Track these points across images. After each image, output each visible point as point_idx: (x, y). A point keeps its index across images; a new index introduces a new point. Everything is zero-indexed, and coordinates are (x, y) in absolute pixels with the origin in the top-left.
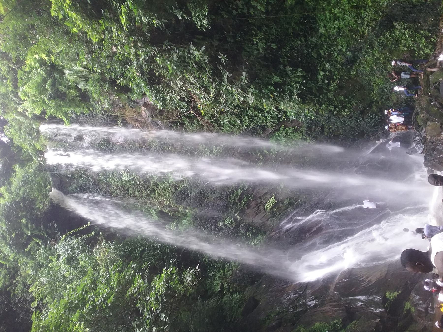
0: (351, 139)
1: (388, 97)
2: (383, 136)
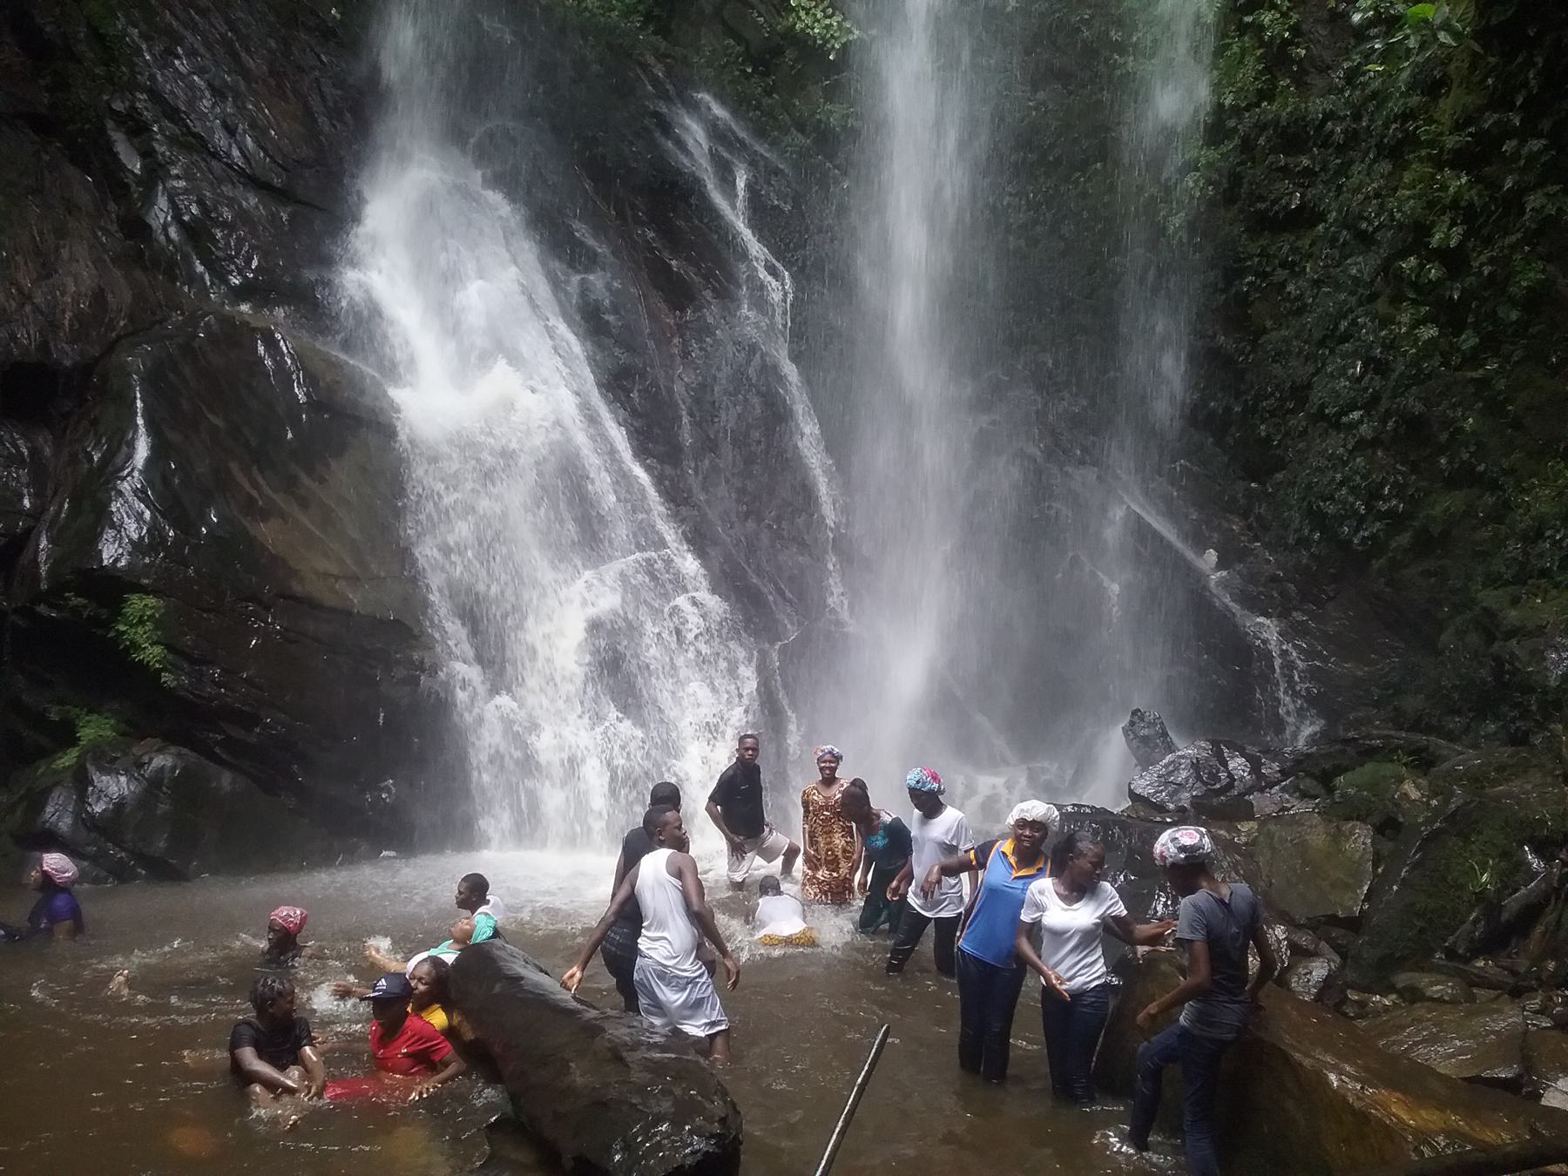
0: (1228, 409)
1: (1544, 573)
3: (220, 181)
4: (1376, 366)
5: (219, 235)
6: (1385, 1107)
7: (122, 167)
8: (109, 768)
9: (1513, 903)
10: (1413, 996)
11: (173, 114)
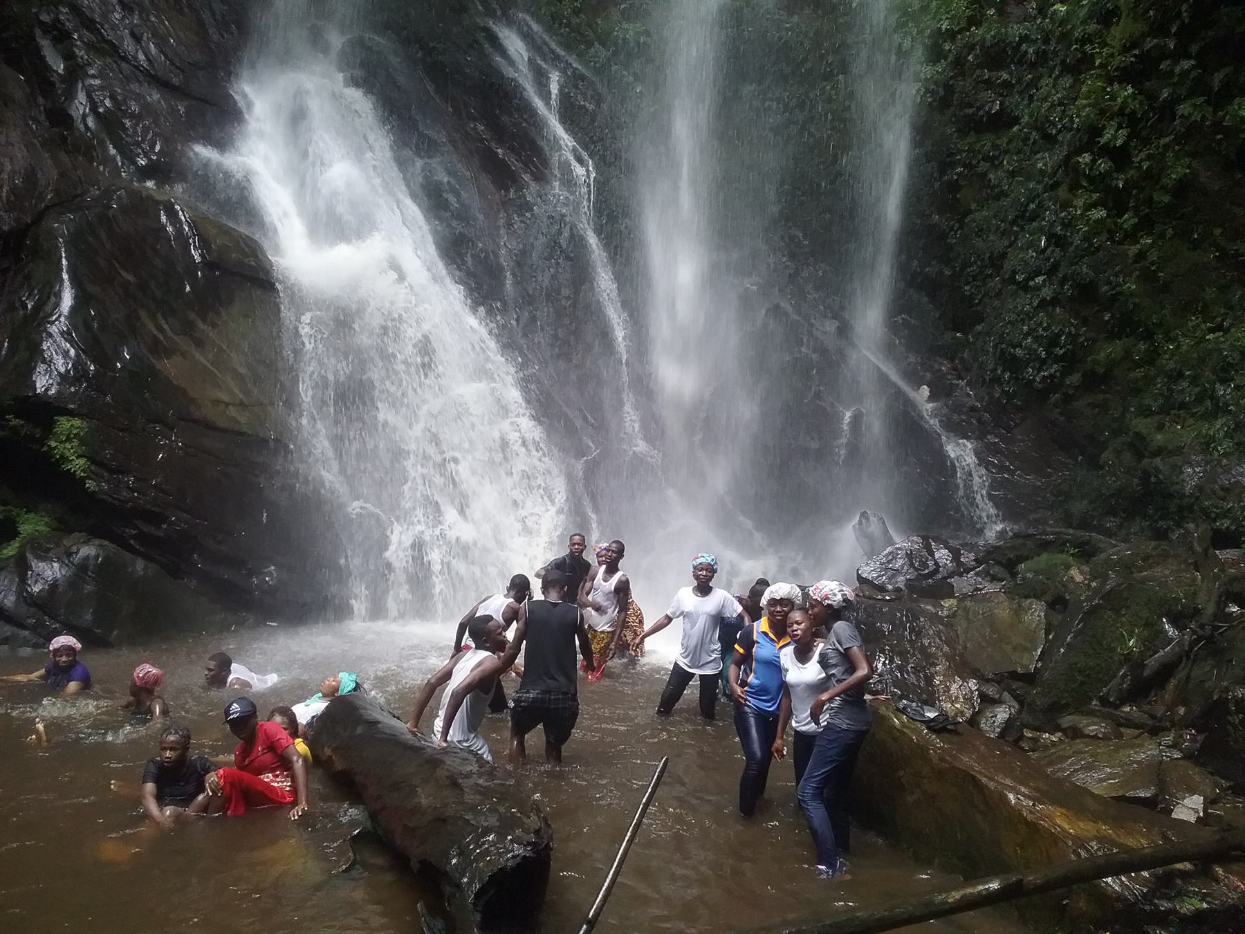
1: (1182, 406)
2: (957, 408)
3: (128, 79)
4: (1057, 241)
5: (128, 124)
6: (1050, 818)
7: (48, 68)
8: (44, 556)
9: (1153, 662)
10: (1075, 733)
11: (89, 24)
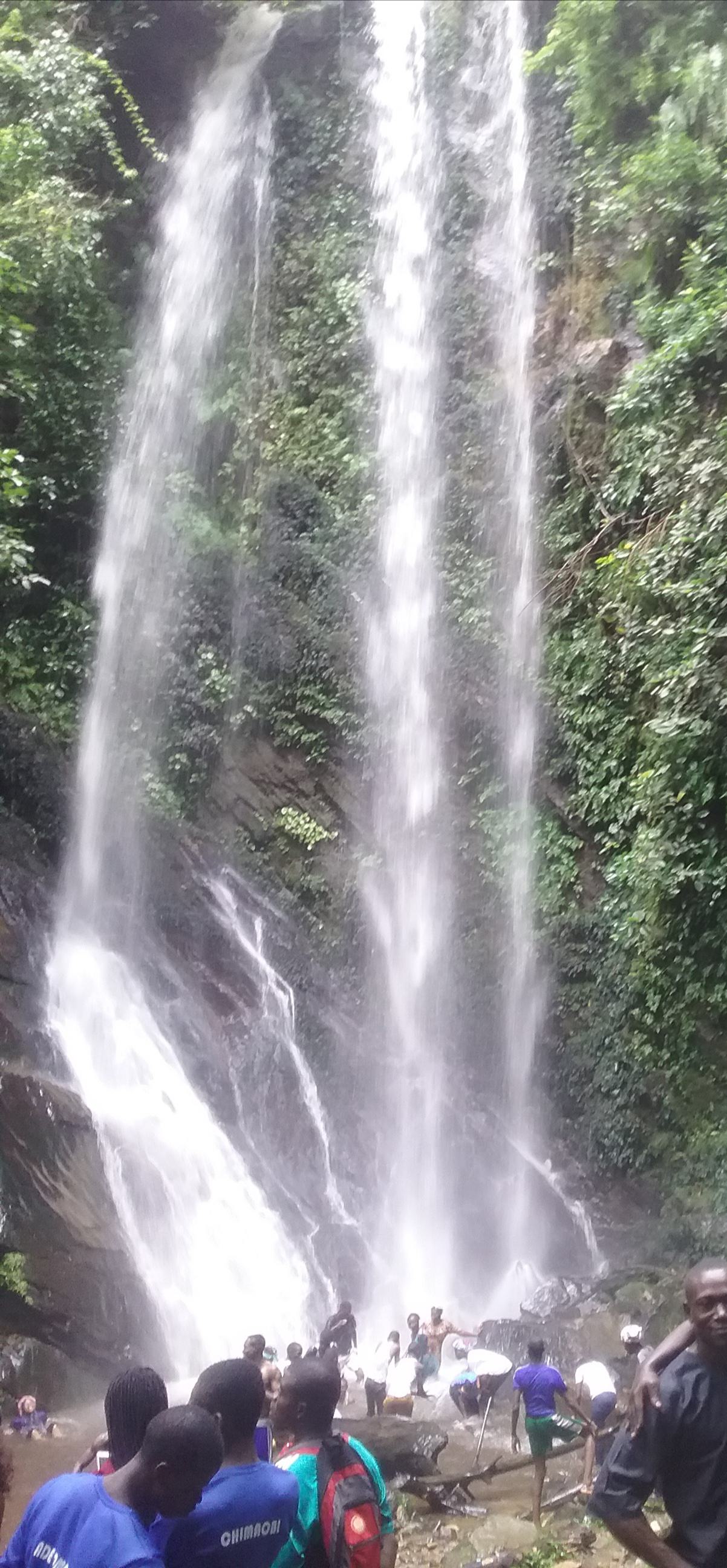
2: (571, 1177)
